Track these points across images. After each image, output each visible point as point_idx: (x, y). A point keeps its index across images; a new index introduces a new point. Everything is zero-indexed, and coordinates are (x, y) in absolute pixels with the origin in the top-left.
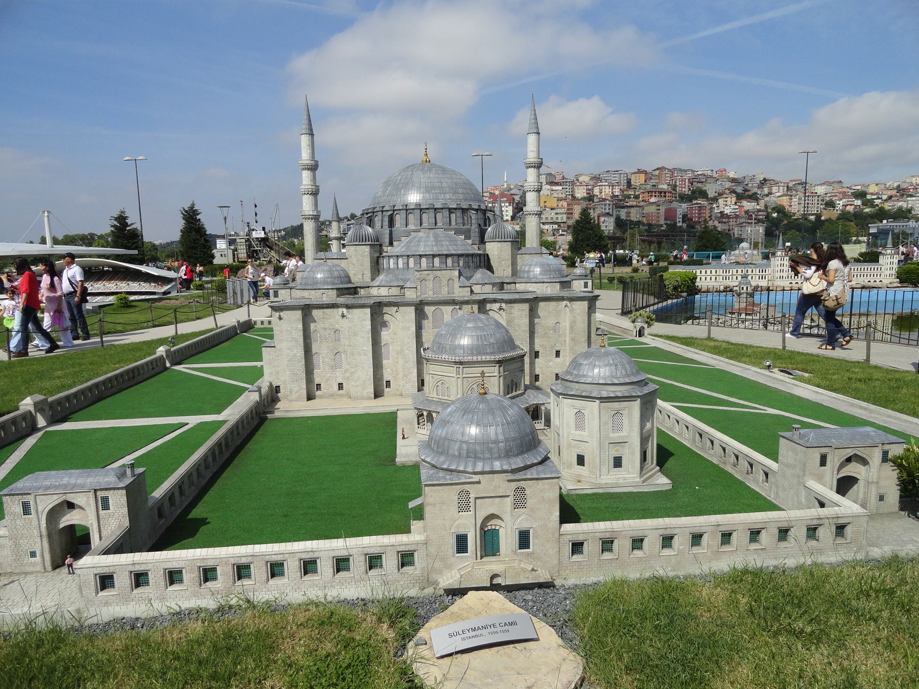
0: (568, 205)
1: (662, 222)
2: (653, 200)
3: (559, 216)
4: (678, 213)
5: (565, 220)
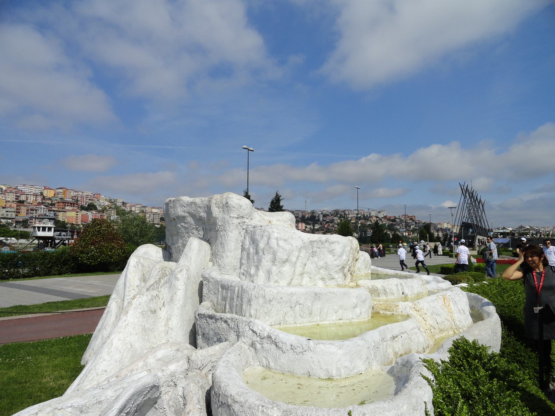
0: (17, 206)
1: (80, 223)
2: (67, 208)
3: (9, 214)
4: (90, 218)
5: (14, 217)
